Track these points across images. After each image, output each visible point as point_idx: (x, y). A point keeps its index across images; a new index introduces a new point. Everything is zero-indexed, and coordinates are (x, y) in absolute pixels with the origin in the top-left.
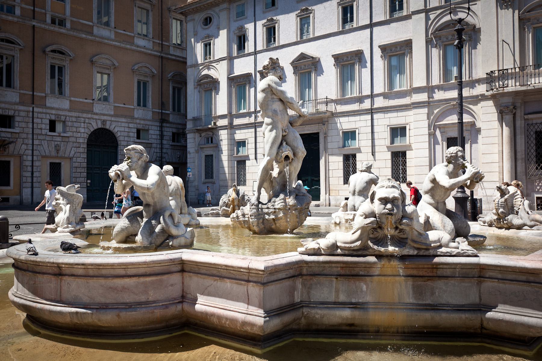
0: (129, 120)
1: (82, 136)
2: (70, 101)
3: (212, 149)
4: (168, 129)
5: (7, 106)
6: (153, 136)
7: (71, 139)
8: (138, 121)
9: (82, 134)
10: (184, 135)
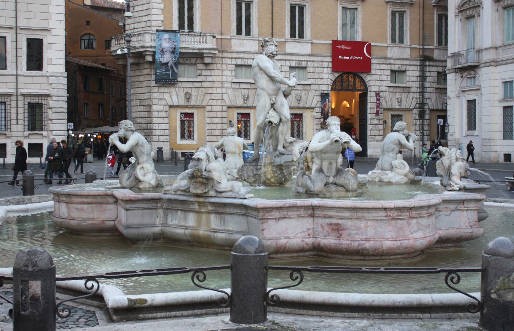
0: (381, 61)
1: (326, 83)
2: (312, 43)
3: (474, 92)
4: (432, 69)
5: (246, 56)
6: (411, 78)
7: (313, 87)
8: (392, 61)
9: (326, 80)
10: (445, 75)
